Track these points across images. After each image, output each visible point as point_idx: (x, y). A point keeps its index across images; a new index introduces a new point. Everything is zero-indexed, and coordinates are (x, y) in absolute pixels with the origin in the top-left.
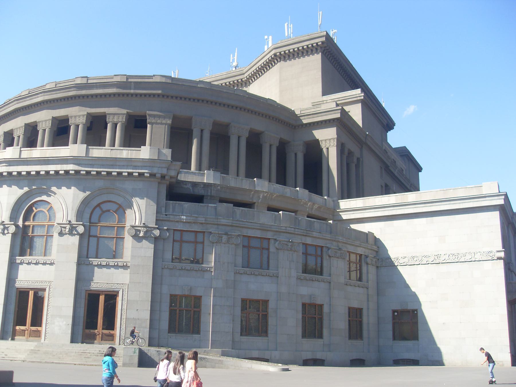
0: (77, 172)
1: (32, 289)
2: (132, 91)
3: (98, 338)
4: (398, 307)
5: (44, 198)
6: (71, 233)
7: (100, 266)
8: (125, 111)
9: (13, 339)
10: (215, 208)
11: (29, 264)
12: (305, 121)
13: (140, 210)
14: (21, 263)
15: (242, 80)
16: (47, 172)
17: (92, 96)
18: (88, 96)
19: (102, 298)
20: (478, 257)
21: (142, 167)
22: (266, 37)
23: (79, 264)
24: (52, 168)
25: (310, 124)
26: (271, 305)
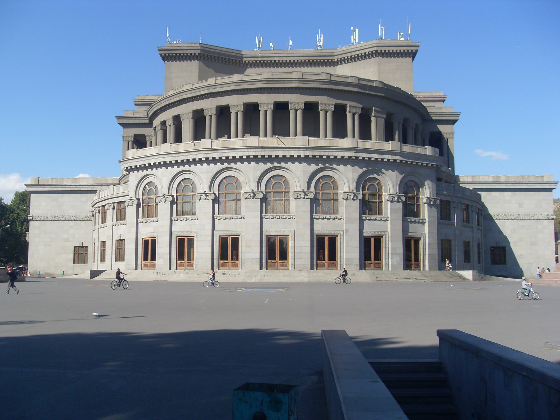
0: (401, 161)
1: (373, 237)
2: (367, 92)
3: (413, 266)
4: (494, 245)
5: (375, 176)
6: (398, 201)
7: (411, 222)
8: (360, 106)
9: (365, 270)
10: (454, 186)
11: (370, 220)
12: (434, 118)
13: (429, 187)
14: (365, 220)
15: (332, 60)
16: (382, 159)
17: (338, 90)
18: (335, 90)
19: (413, 242)
20: (541, 217)
21: (433, 161)
22: (352, 28)
23: (403, 221)
24: (386, 157)
25: (436, 120)
26: (471, 244)
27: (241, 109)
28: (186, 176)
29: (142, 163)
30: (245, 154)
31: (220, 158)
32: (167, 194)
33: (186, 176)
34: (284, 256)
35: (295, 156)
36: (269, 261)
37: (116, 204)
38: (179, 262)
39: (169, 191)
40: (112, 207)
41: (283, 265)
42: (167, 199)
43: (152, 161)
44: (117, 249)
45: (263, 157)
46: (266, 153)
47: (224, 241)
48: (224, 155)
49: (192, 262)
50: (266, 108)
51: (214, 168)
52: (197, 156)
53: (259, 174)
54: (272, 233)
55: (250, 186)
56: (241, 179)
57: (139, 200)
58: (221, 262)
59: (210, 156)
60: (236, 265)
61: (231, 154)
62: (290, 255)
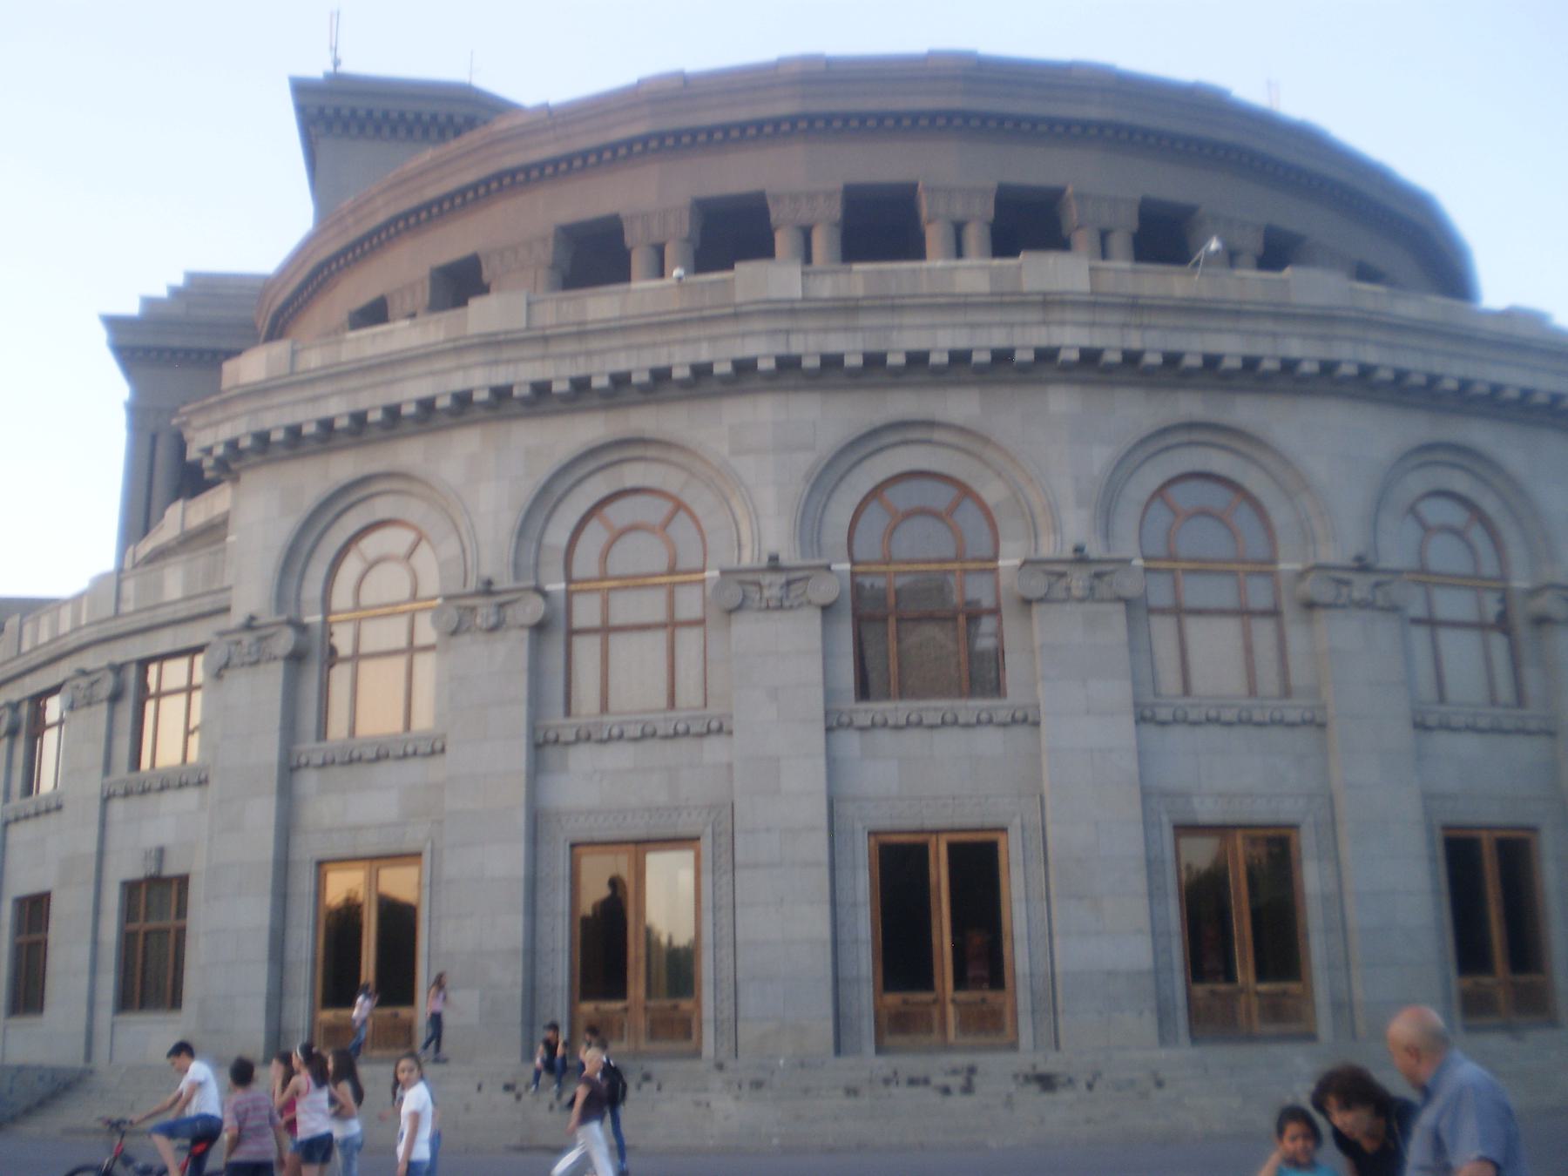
27: (835, 210)
28: (633, 475)
29: (337, 408)
30: (1027, 338)
31: (874, 361)
32: (505, 581)
33: (633, 475)
34: (1280, 950)
35: (1308, 367)
36: (1201, 990)
37: (132, 674)
38: (587, 1007)
39: (516, 566)
40: (106, 686)
41: (1276, 1010)
42: (509, 612)
43: (409, 391)
44: (127, 941)
45: (1132, 358)
46: (1152, 343)
47: (900, 865)
48: (900, 342)
49: (686, 1004)
50: (958, 211)
51: (827, 419)
52: (720, 354)
53: (1100, 458)
54: (1207, 811)
55: (1056, 529)
56: (992, 492)
57: (301, 628)
58: (893, 999)
59: (809, 345)
60: (989, 1024)
61: (941, 341)
62: (1317, 947)
